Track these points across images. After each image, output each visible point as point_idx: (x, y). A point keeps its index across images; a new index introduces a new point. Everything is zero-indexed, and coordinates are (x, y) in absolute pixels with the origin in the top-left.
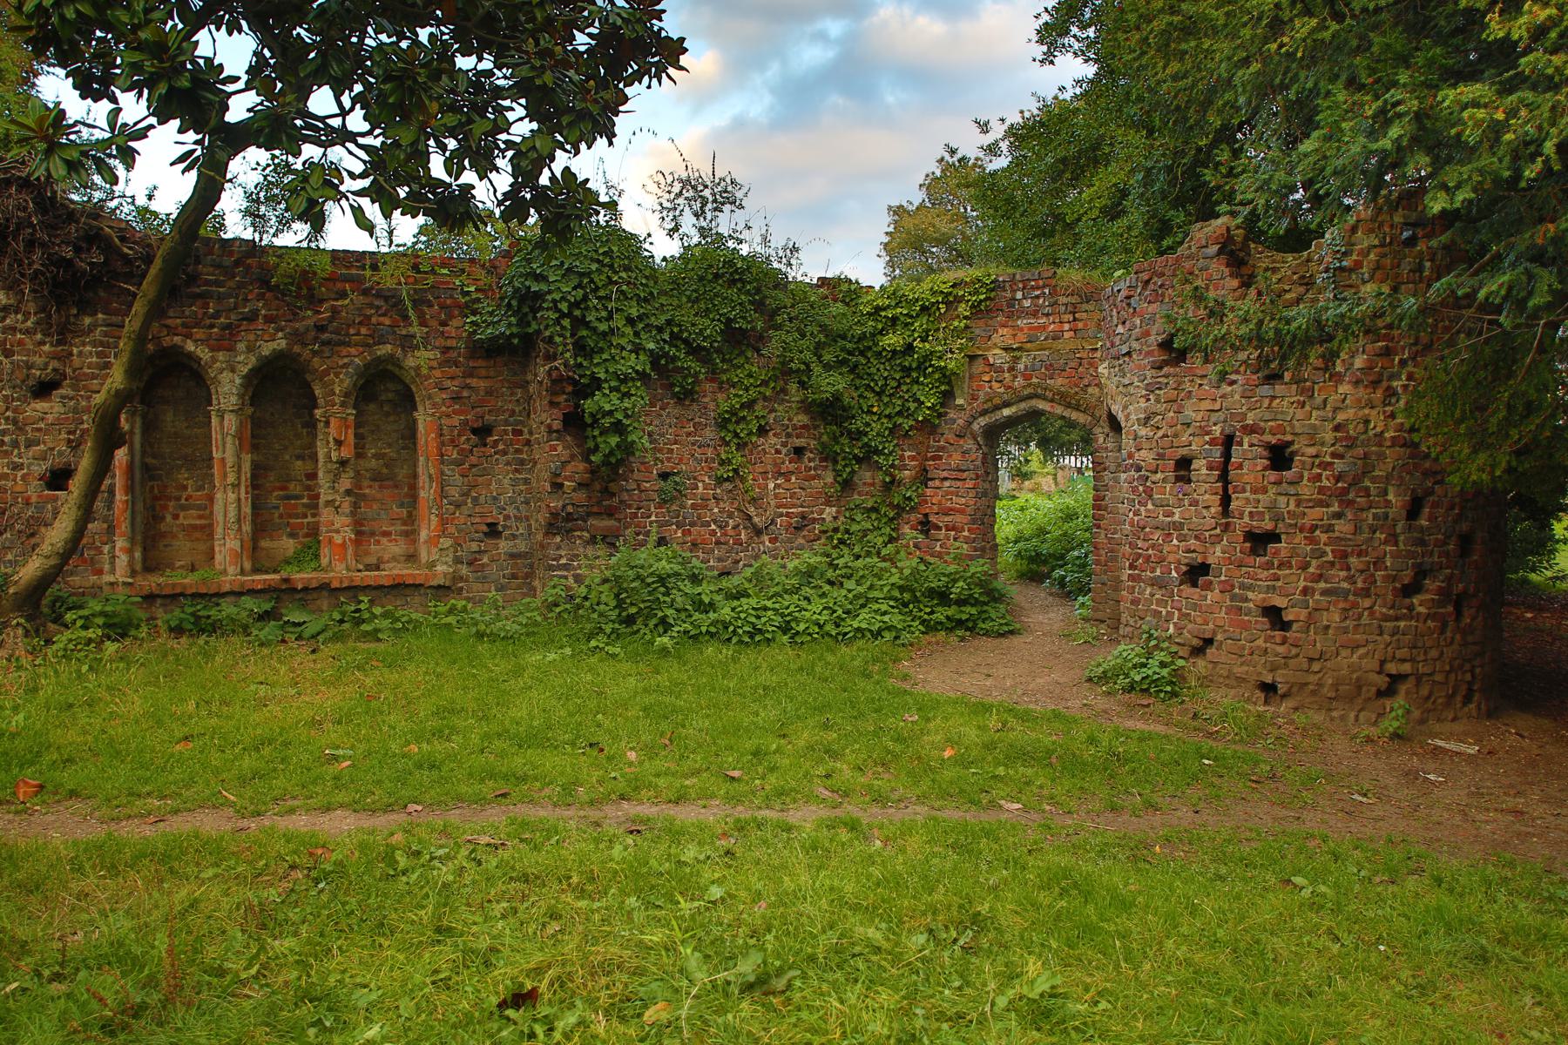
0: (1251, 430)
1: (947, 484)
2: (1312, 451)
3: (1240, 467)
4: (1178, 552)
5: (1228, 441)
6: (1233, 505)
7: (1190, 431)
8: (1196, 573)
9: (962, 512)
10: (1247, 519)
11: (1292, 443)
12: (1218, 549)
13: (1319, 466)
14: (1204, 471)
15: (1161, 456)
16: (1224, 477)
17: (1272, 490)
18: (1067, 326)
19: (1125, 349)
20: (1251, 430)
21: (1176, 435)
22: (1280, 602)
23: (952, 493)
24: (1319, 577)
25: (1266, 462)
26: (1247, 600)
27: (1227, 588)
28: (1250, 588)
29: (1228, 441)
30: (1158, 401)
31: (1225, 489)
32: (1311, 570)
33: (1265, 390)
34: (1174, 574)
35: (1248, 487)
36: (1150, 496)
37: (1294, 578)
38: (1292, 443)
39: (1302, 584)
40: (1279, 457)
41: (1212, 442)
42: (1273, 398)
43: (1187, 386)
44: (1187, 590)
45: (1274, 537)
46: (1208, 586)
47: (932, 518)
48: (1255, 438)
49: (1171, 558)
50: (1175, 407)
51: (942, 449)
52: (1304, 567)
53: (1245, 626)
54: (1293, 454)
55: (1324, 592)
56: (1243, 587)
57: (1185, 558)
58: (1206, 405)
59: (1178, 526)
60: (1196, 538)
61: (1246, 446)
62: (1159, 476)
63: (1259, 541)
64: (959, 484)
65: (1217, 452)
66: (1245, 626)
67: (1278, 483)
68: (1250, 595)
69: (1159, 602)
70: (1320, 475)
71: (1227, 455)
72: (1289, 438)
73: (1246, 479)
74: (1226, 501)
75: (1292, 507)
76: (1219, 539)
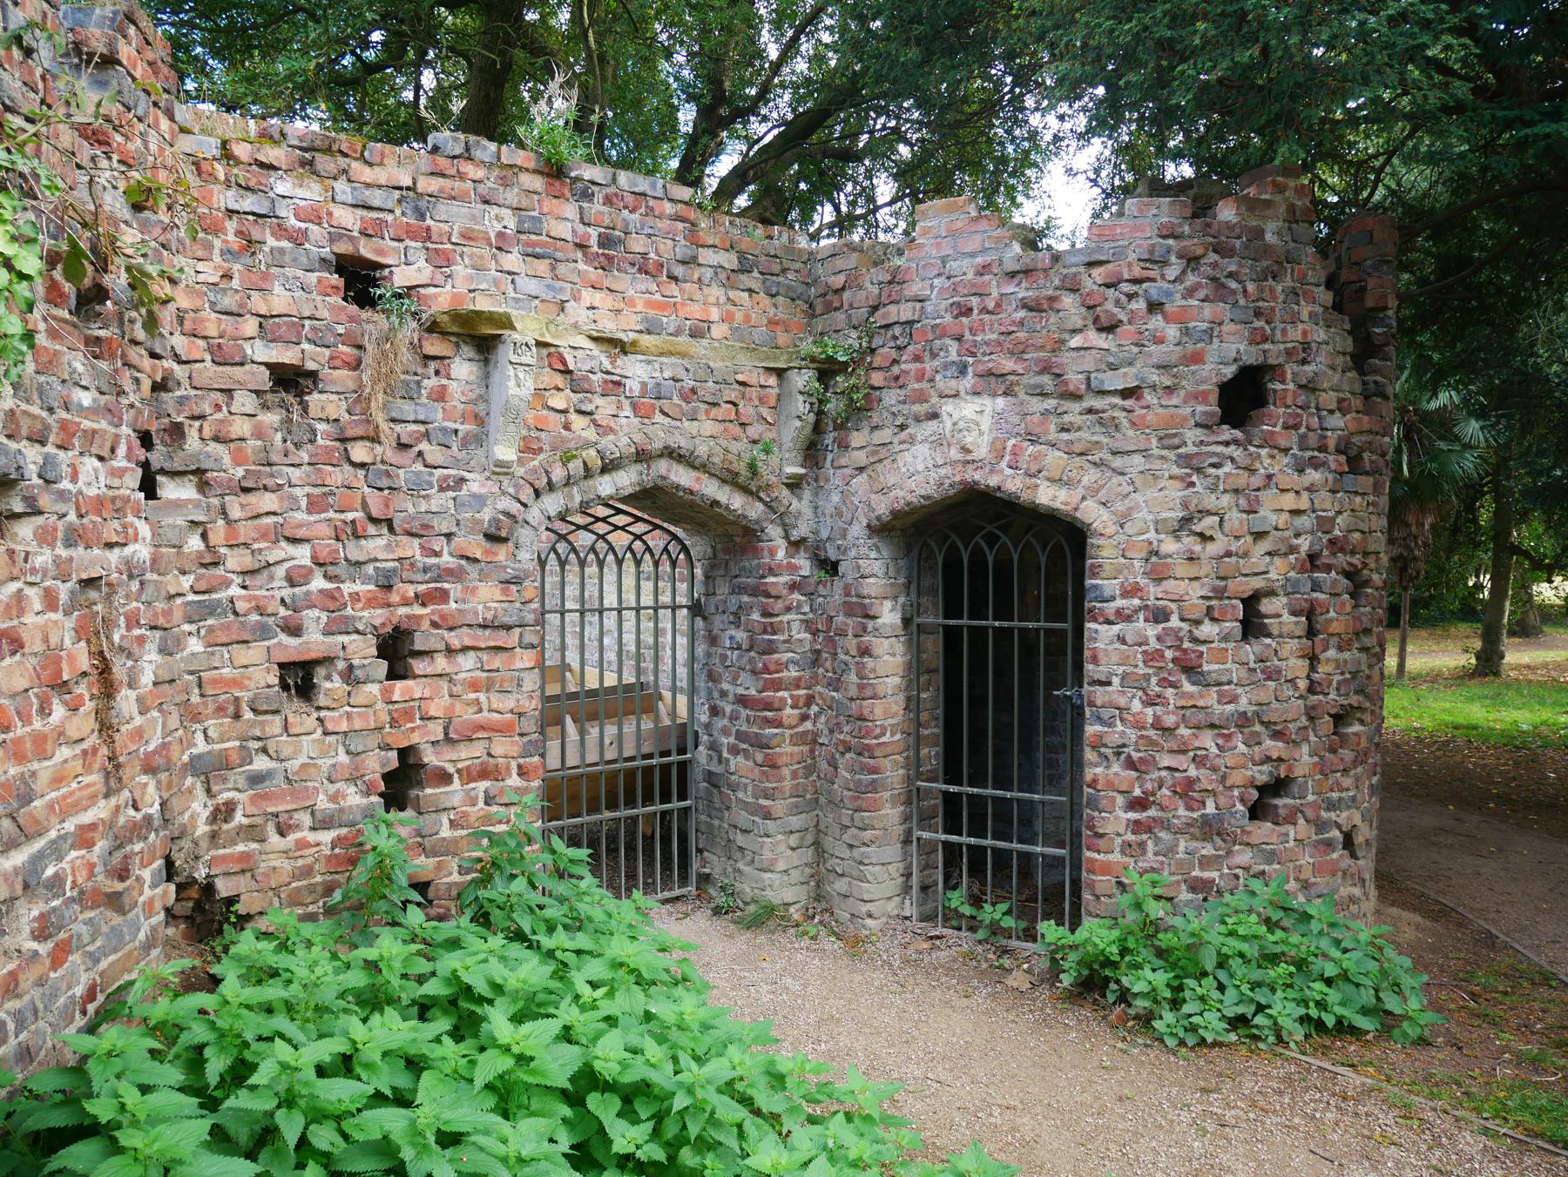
1: (467, 662)
4: (1245, 764)
7: (1265, 545)
9: (504, 730)
15: (1220, 593)
18: (715, 314)
23: (475, 686)
35: (1334, 641)
44: (1263, 831)
47: (430, 758)
51: (454, 574)
58: (1289, 501)
59: (1243, 721)
64: (497, 661)
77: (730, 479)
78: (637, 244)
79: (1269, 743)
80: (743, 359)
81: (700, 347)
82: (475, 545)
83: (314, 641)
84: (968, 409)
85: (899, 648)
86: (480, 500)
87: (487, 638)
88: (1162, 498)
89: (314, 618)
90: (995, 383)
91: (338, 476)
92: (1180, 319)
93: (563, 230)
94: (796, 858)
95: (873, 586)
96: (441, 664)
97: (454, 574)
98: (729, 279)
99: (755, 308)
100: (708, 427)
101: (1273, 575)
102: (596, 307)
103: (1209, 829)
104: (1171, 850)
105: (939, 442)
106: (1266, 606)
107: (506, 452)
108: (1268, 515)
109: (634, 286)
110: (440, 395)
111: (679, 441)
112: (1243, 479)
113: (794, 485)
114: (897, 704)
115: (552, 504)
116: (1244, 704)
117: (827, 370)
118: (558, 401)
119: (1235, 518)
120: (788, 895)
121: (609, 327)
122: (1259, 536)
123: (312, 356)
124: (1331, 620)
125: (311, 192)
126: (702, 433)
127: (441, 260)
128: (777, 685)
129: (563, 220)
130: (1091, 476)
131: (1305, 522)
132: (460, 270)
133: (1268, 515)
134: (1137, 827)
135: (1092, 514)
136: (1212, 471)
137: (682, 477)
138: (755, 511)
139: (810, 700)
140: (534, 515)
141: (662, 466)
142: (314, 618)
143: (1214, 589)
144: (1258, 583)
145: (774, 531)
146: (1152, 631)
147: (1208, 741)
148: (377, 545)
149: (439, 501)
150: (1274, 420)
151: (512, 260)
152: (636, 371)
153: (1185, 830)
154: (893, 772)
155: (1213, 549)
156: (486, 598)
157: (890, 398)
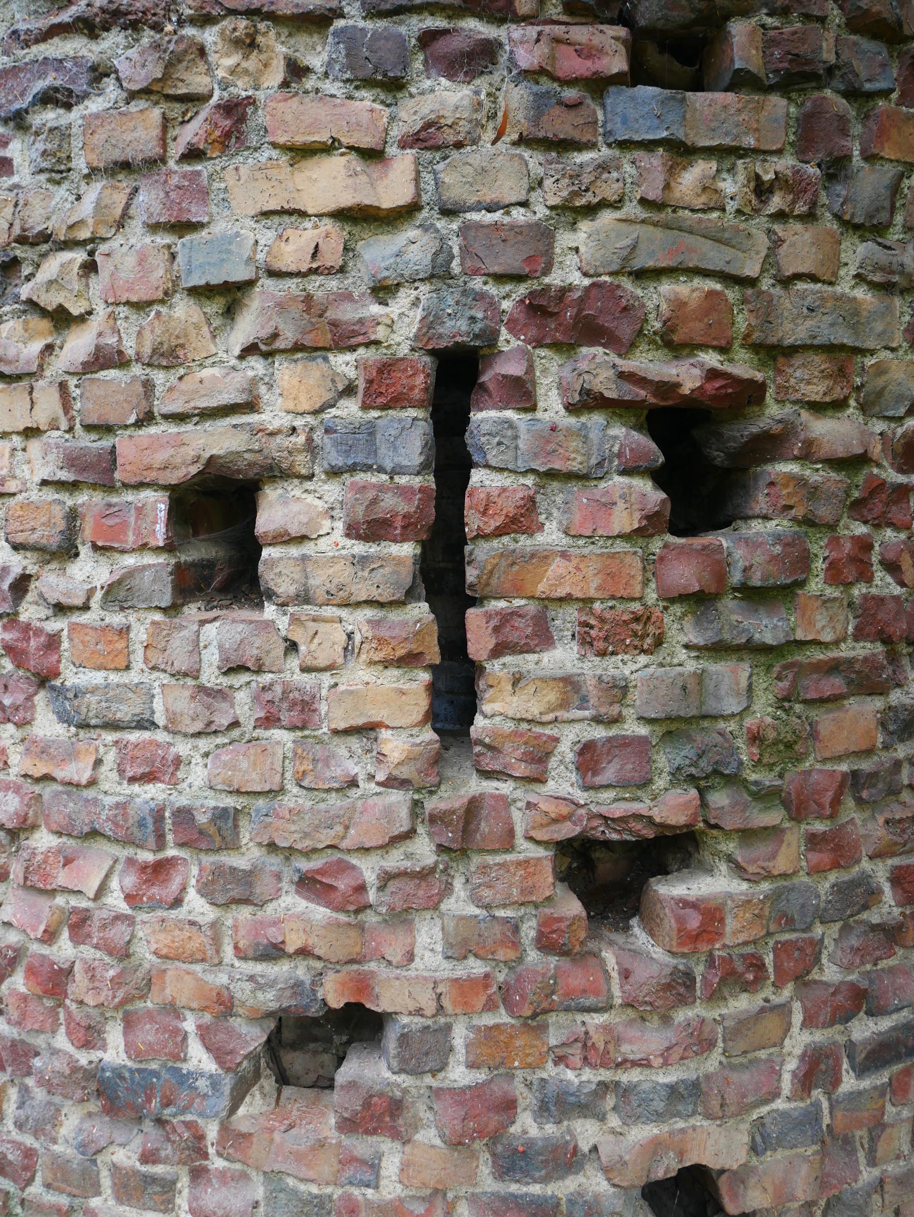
2: (835, 432)
3: (523, 520)
4: (223, 956)
5: (456, 377)
6: (498, 711)
7: (248, 326)
10: (563, 782)
11: (751, 394)
12: (428, 936)
13: (857, 508)
14: (334, 541)
15: (98, 472)
17: (681, 631)
21: (168, 356)
24: (860, 1000)
25: (653, 496)
26: (566, 1159)
27: (483, 1120)
28: (584, 1106)
29: (456, 377)
30: (57, 170)
31: (453, 642)
32: (830, 973)
33: (642, 108)
34: (199, 1059)
35: (566, 619)
36: (44, 679)
37: (771, 1024)
38: (751, 394)
39: (799, 1040)
40: (699, 460)
41: (381, 389)
42: (681, 152)
45: (673, 849)
46: (381, 1115)
48: (598, 365)
50: (149, 200)
52: (799, 965)
54: (770, 445)
56: (559, 1105)
57: (262, 988)
58: (330, 183)
60: (309, 884)
61: (551, 405)
62: (88, 572)
63: (612, 874)
65: (407, 436)
67: (700, 601)
68: (586, 1132)
70: (865, 545)
71: (451, 461)
72: (743, 366)
73: (556, 578)
74: (455, 697)
75: (763, 711)
76: (421, 889)
79: (292, 902)
101: (272, 416)
106: (274, 511)
112: (141, 130)
116: (197, 785)
119: (132, 255)
124: (542, 557)
131: (410, 247)
133: (235, 235)
136: (50, 116)
143: (72, 461)
144: (221, 440)
155: (78, 345)
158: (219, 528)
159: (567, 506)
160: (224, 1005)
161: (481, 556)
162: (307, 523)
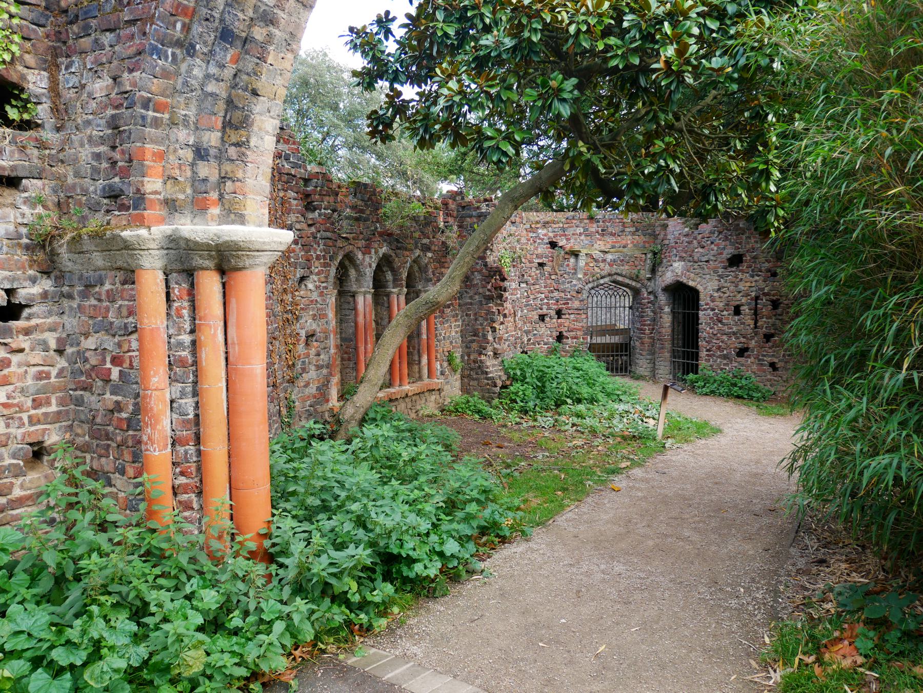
0: (765, 294)
1: (572, 316)
4: (735, 343)
6: (759, 324)
8: (742, 352)
9: (579, 330)
15: (727, 305)
16: (756, 314)
19: (704, 259)
20: (765, 294)
22: (776, 360)
41: (752, 299)
43: (740, 276)
44: (740, 359)
45: (772, 335)
46: (749, 357)
47: (565, 334)
49: (732, 346)
51: (570, 299)
53: (764, 371)
55: (789, 355)
57: (740, 346)
58: (748, 284)
59: (734, 333)
66: (764, 371)
69: (724, 365)
71: (756, 304)
74: (756, 323)
76: (752, 338)
77: (631, 279)
78: (610, 230)
80: (636, 252)
81: (625, 250)
82: (574, 294)
83: (545, 311)
84: (676, 265)
85: (670, 317)
86: (575, 285)
87: (576, 312)
88: (714, 284)
89: (545, 307)
90: (682, 259)
91: (549, 281)
92: (717, 245)
93: (593, 230)
94: (649, 366)
95: (662, 303)
96: (567, 316)
97: (570, 299)
98: (633, 234)
99: (639, 239)
100: (627, 267)
102: (600, 245)
103: (725, 357)
104: (715, 361)
105: (673, 271)
106: (742, 308)
107: (580, 276)
108: (741, 286)
109: (610, 239)
110: (568, 265)
111: (619, 271)
112: (734, 279)
113: (649, 279)
114: (669, 330)
115: (590, 285)
116: (734, 329)
117: (655, 254)
118: (592, 265)
119: (732, 288)
120: (646, 374)
121: (603, 248)
122: (740, 292)
123: (544, 260)
125: (545, 231)
126: (625, 269)
127: (568, 240)
128: (645, 325)
129: (593, 228)
130: (699, 279)
131: (754, 289)
132: (572, 241)
133: (741, 286)
134: (707, 355)
135: (699, 288)
137: (620, 279)
138: (639, 285)
139: (653, 329)
140: (586, 288)
141: (615, 277)
142: (545, 307)
144: (738, 303)
145: (644, 290)
146: (711, 313)
147: (725, 338)
148: (556, 294)
149: (567, 285)
150: (744, 266)
151: (583, 237)
152: (609, 257)
153: (720, 357)
154: (668, 345)
156: (576, 304)
157: (665, 261)
158: (737, 311)
159: (765, 308)
160: (736, 348)
161: (759, 312)
162: (745, 309)
